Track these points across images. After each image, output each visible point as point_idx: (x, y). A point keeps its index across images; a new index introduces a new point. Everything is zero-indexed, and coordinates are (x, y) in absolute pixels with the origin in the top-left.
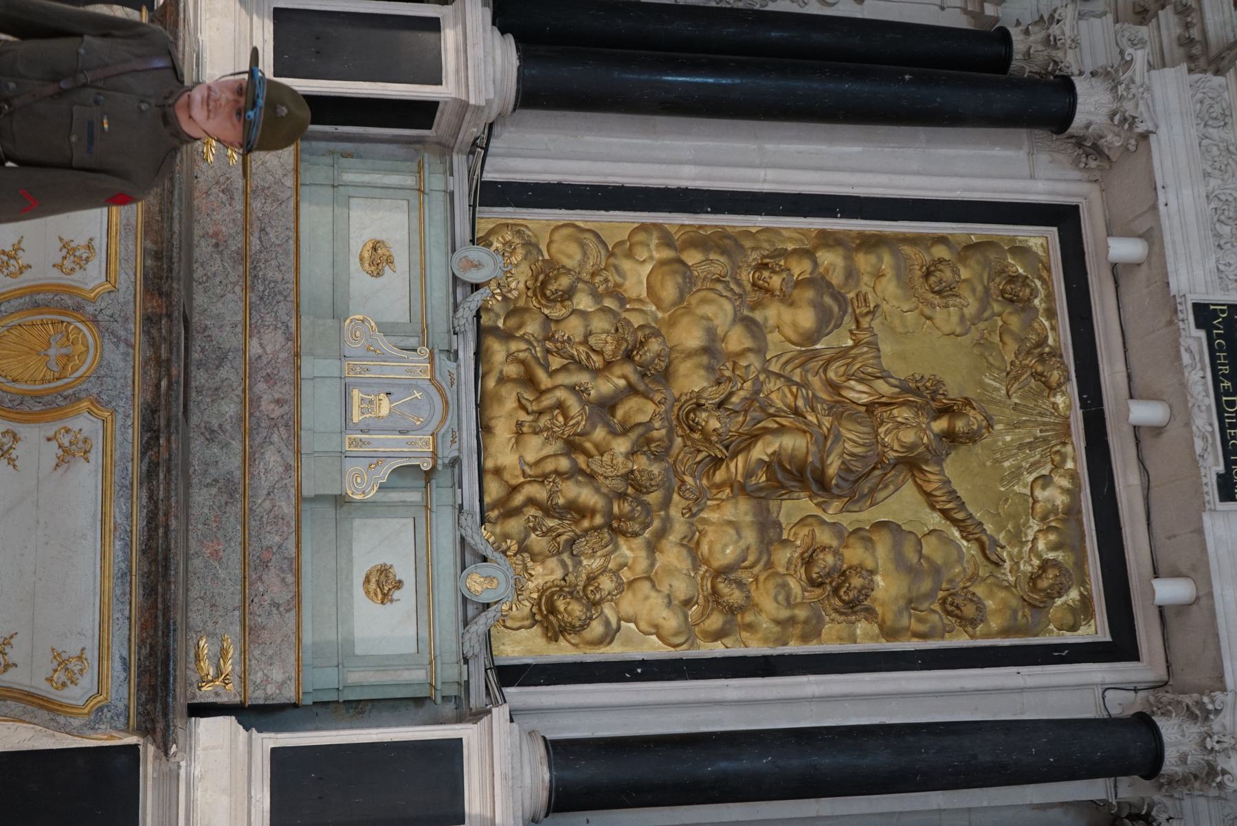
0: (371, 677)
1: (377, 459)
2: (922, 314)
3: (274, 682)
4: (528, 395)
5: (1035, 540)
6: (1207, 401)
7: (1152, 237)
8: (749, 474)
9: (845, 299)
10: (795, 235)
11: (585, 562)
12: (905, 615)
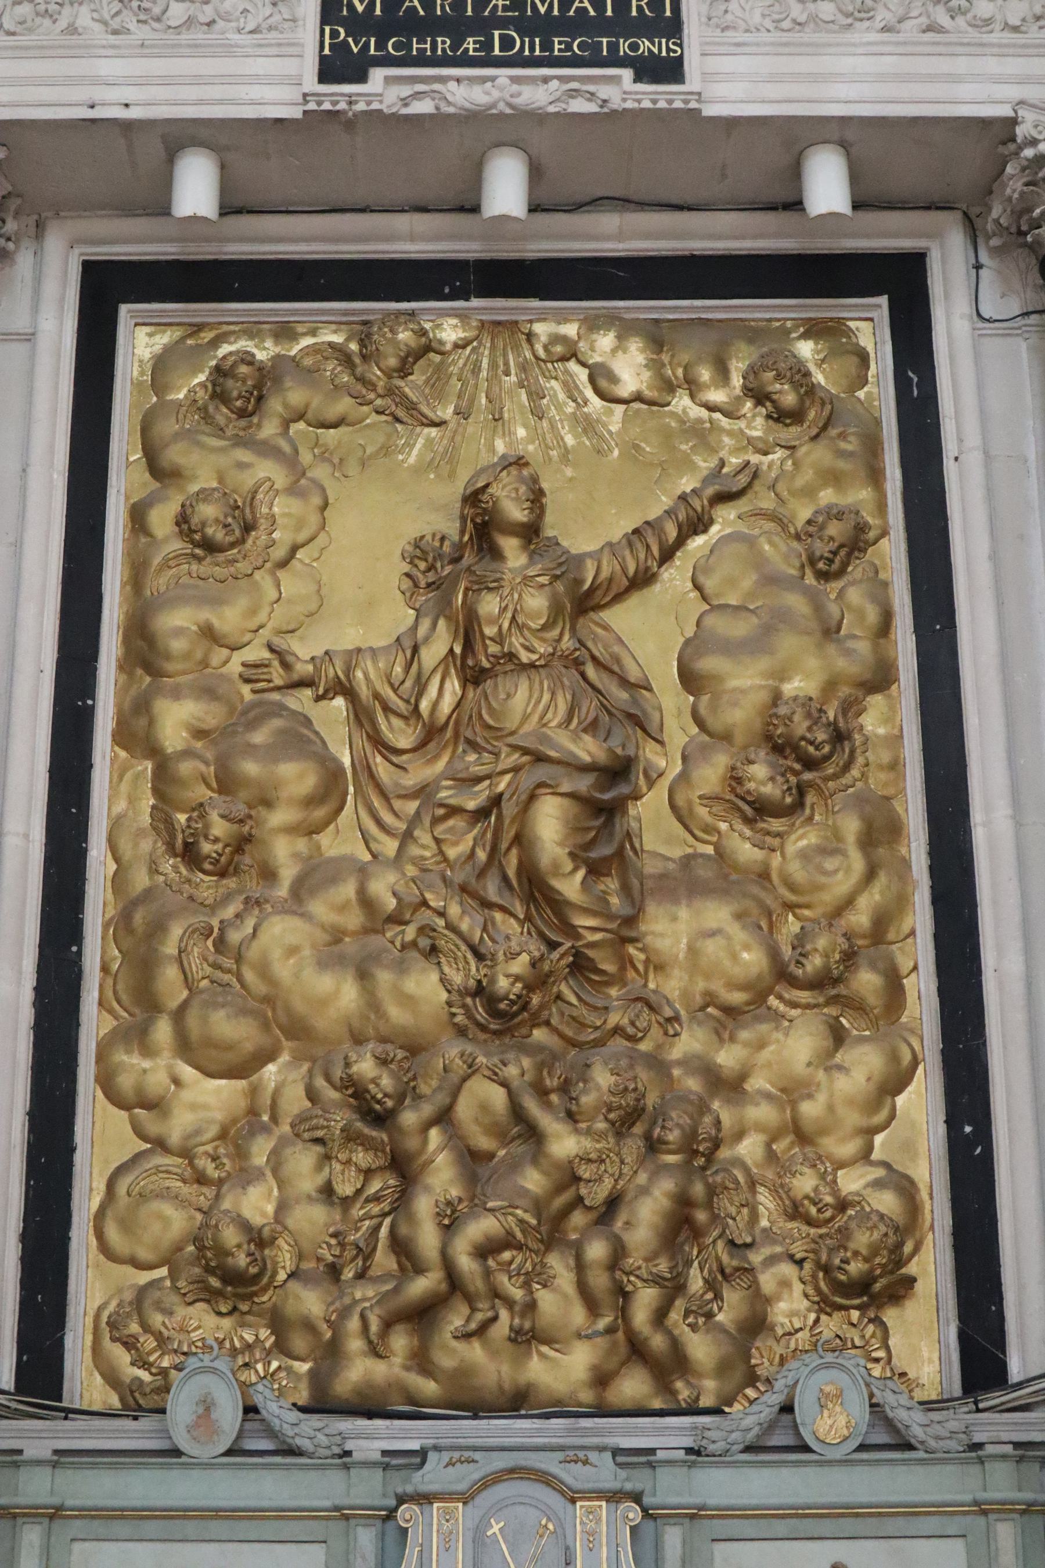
2: (283, 564)
4: (456, 1319)
5: (711, 408)
6: (503, 81)
7: (178, 137)
8: (602, 910)
9: (253, 705)
10: (124, 787)
11: (764, 1223)
12: (851, 644)
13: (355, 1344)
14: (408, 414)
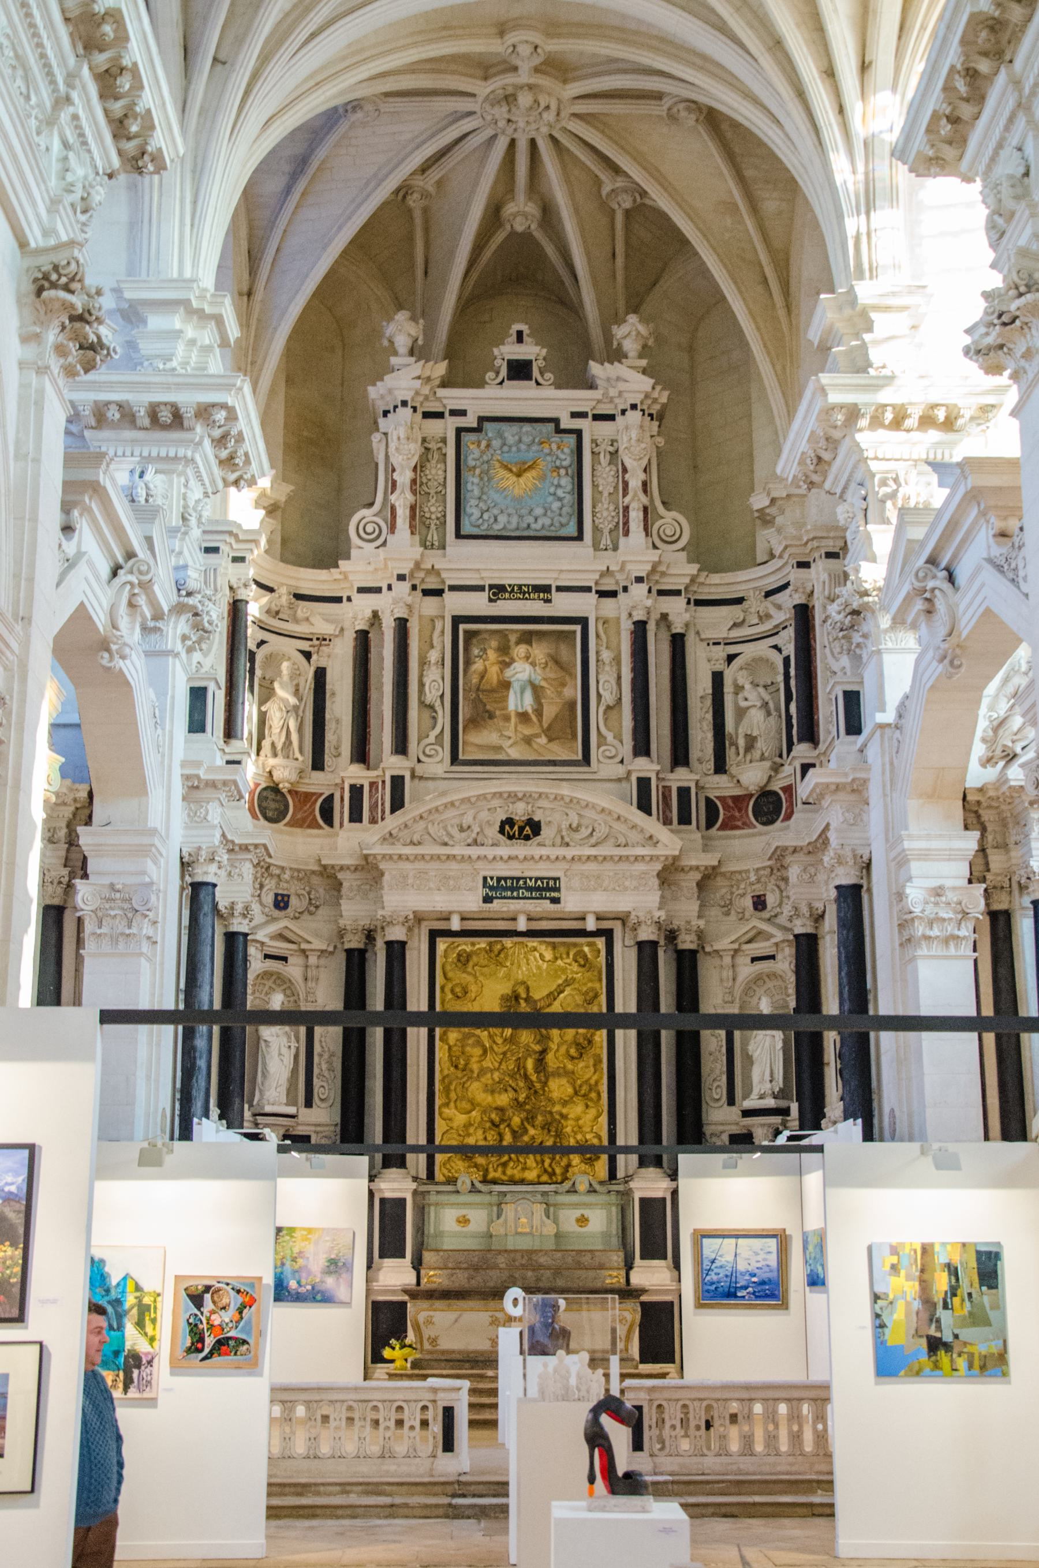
0: (614, 1226)
1: (543, 1223)
3: (617, 1258)
4: (511, 1164)
7: (450, 913)
8: (540, 1081)
13: (491, 1170)
14: (502, 965)
